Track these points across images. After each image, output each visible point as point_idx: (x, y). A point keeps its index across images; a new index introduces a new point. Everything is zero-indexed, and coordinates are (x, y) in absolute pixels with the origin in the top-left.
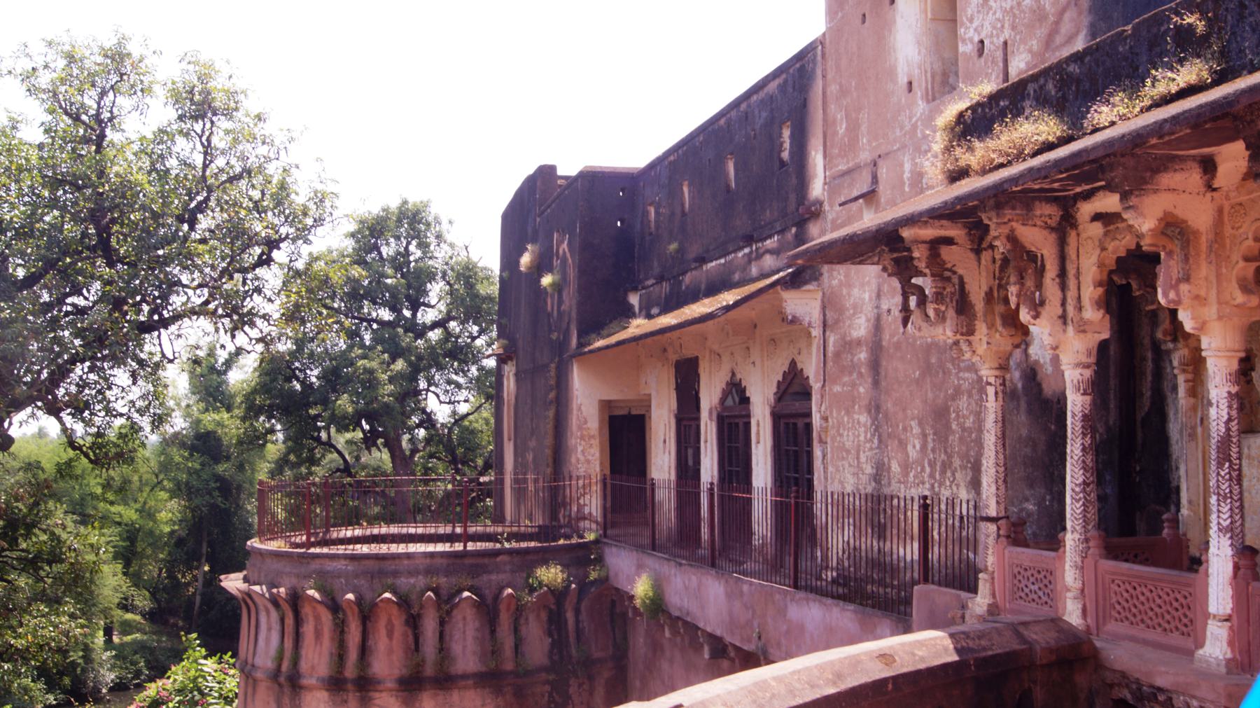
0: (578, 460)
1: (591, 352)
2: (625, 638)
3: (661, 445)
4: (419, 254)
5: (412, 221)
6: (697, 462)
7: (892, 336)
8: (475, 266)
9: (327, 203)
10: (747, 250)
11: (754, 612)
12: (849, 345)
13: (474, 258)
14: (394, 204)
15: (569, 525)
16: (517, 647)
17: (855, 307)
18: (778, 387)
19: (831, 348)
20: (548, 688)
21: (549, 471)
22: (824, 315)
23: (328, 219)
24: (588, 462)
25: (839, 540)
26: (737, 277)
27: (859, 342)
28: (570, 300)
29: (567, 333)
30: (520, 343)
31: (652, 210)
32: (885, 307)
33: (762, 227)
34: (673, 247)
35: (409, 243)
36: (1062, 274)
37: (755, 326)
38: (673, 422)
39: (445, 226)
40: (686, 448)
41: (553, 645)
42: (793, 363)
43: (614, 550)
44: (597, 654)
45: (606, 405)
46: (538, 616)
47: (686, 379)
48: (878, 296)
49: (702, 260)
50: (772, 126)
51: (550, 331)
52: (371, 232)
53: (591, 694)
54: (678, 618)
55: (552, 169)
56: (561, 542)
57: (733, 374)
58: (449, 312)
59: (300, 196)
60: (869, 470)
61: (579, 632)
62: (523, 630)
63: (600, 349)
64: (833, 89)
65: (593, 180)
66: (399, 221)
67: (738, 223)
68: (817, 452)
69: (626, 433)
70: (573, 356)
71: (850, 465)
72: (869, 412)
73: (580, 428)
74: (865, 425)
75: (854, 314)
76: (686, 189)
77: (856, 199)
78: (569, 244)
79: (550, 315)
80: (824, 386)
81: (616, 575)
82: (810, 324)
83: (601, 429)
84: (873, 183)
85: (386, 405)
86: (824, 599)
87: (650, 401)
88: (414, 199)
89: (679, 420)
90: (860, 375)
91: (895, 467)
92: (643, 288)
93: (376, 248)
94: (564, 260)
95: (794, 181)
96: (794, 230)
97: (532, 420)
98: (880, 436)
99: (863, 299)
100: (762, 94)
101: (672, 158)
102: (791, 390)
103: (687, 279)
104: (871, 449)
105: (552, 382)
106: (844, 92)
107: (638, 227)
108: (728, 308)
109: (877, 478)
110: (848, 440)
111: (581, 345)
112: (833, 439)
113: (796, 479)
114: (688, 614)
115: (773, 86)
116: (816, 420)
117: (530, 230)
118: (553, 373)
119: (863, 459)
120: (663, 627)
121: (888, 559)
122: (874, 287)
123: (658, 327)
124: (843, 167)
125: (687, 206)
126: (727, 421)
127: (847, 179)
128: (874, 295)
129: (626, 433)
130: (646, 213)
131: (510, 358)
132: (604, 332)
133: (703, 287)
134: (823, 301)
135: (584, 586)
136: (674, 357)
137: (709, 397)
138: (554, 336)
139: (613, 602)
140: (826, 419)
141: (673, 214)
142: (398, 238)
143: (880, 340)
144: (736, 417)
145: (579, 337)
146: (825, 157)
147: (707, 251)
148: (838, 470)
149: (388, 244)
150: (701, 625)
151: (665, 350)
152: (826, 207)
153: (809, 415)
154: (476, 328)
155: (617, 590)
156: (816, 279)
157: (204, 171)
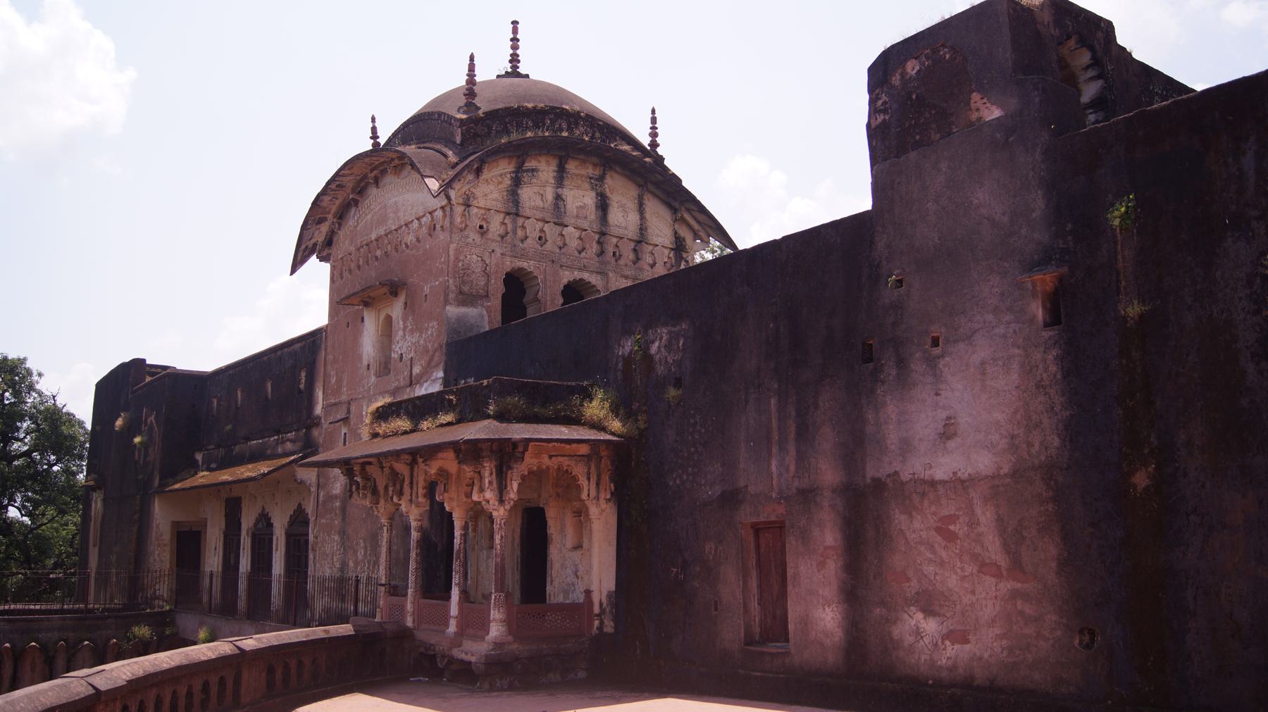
6: (237, 562)
12: (330, 498)
26: (269, 452)
31: (215, 401)
34: (229, 427)
36: (411, 483)
42: (300, 505)
45: (176, 524)
49: (248, 439)
63: (177, 490)
64: (330, 357)
68: (311, 556)
69: (188, 543)
89: (226, 536)
91: (351, 564)
94: (151, 428)
100: (291, 349)
103: (237, 448)
109: (341, 570)
111: (162, 485)
116: (311, 538)
129: (188, 543)
131: (100, 488)
137: (248, 521)
138: (140, 477)
154: (53, 457)
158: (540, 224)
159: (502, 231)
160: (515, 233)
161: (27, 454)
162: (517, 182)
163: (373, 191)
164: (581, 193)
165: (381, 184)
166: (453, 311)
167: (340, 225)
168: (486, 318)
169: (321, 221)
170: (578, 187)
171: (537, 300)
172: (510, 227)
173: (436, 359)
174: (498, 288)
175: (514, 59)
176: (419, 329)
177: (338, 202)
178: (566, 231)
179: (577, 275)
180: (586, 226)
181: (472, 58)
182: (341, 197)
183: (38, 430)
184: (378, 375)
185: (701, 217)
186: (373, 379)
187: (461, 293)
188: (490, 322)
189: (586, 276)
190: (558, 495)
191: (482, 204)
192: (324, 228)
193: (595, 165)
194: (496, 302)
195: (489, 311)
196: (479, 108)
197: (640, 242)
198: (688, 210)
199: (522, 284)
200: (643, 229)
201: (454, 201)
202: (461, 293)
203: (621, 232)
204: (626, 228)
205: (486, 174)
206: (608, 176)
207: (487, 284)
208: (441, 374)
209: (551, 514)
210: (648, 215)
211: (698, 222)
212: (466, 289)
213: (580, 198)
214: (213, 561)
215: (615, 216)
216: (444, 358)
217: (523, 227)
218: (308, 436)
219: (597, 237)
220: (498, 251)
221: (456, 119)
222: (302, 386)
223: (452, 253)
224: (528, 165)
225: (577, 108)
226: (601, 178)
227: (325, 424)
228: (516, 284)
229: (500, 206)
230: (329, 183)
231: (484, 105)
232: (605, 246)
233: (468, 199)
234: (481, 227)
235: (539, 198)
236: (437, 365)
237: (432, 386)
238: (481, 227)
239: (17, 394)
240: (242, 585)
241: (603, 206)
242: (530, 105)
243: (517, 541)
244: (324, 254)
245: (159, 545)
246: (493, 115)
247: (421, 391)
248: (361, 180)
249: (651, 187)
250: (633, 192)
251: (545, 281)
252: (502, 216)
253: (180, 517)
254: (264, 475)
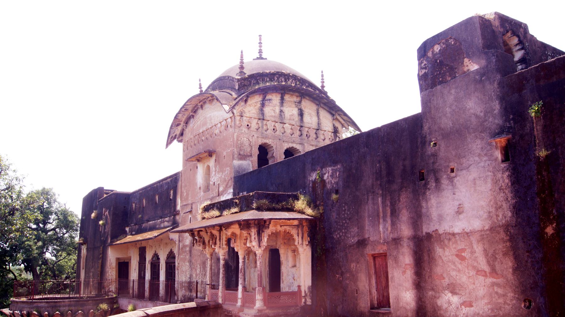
6: (145, 275)
12: (185, 246)
25: (181, 293)
27: (187, 246)
28: (108, 229)
29: (107, 238)
31: (134, 205)
34: (140, 216)
36: (220, 239)
42: (171, 250)
45: (118, 259)
49: (148, 221)
50: (168, 190)
51: (101, 237)
60: (188, 276)
63: (118, 244)
64: (183, 184)
68: (176, 272)
69: (123, 267)
73: (110, 266)
76: (144, 201)
78: (109, 212)
79: (101, 232)
89: (140, 263)
91: (194, 275)
94: (107, 217)
100: (166, 181)
103: (144, 225)
106: (186, 186)
109: (190, 278)
110: (184, 269)
111: (111, 242)
115: (169, 180)
124: (185, 203)
129: (123, 267)
131: (85, 244)
132: (119, 238)
136: (139, 246)
137: (149, 257)
138: (102, 239)
141: (140, 207)
153: (175, 263)
158: (273, 123)
159: (257, 127)
160: (263, 127)
161: (54, 229)
162: (263, 105)
163: (200, 111)
164: (291, 109)
165: (204, 108)
166: (236, 163)
167: (186, 126)
168: (251, 165)
169: (178, 125)
170: (290, 106)
171: (273, 157)
172: (260, 125)
173: (229, 184)
174: (256, 152)
175: (260, 52)
176: (221, 171)
177: (185, 117)
178: (285, 126)
179: (291, 145)
180: (294, 123)
181: (242, 52)
182: (187, 114)
183: (58, 219)
184: (205, 192)
185: (345, 118)
186: (202, 193)
187: (240, 154)
188: (253, 167)
189: (295, 146)
190: (285, 243)
191: (248, 115)
192: (180, 128)
193: (297, 96)
194: (255, 158)
195: (252, 162)
196: (245, 74)
197: (318, 130)
198: (339, 115)
199: (266, 150)
200: (319, 124)
201: (235, 115)
202: (240, 154)
203: (309, 125)
204: (311, 124)
205: (250, 102)
206: (303, 101)
207: (251, 150)
208: (232, 191)
209: (282, 252)
210: (321, 117)
211: (344, 120)
212: (242, 153)
213: (291, 111)
214: (134, 275)
215: (307, 118)
216: (233, 184)
217: (266, 125)
218: (174, 219)
219: (299, 128)
220: (256, 136)
221: (236, 79)
222: (171, 197)
223: (235, 137)
224: (267, 97)
225: (288, 72)
226: (300, 102)
227: (182, 214)
228: (264, 150)
229: (256, 116)
230: (181, 109)
231: (248, 72)
232: (303, 132)
233: (242, 113)
234: (248, 125)
235: (273, 112)
236: (230, 187)
237: (228, 196)
238: (248, 125)
239: (49, 203)
240: (147, 285)
241: (301, 114)
242: (268, 71)
243: (267, 264)
244: (180, 139)
246: (252, 76)
247: (223, 198)
248: (195, 107)
249: (322, 105)
250: (314, 107)
251: (276, 149)
252: (257, 120)
253: (120, 256)
254: (156, 237)
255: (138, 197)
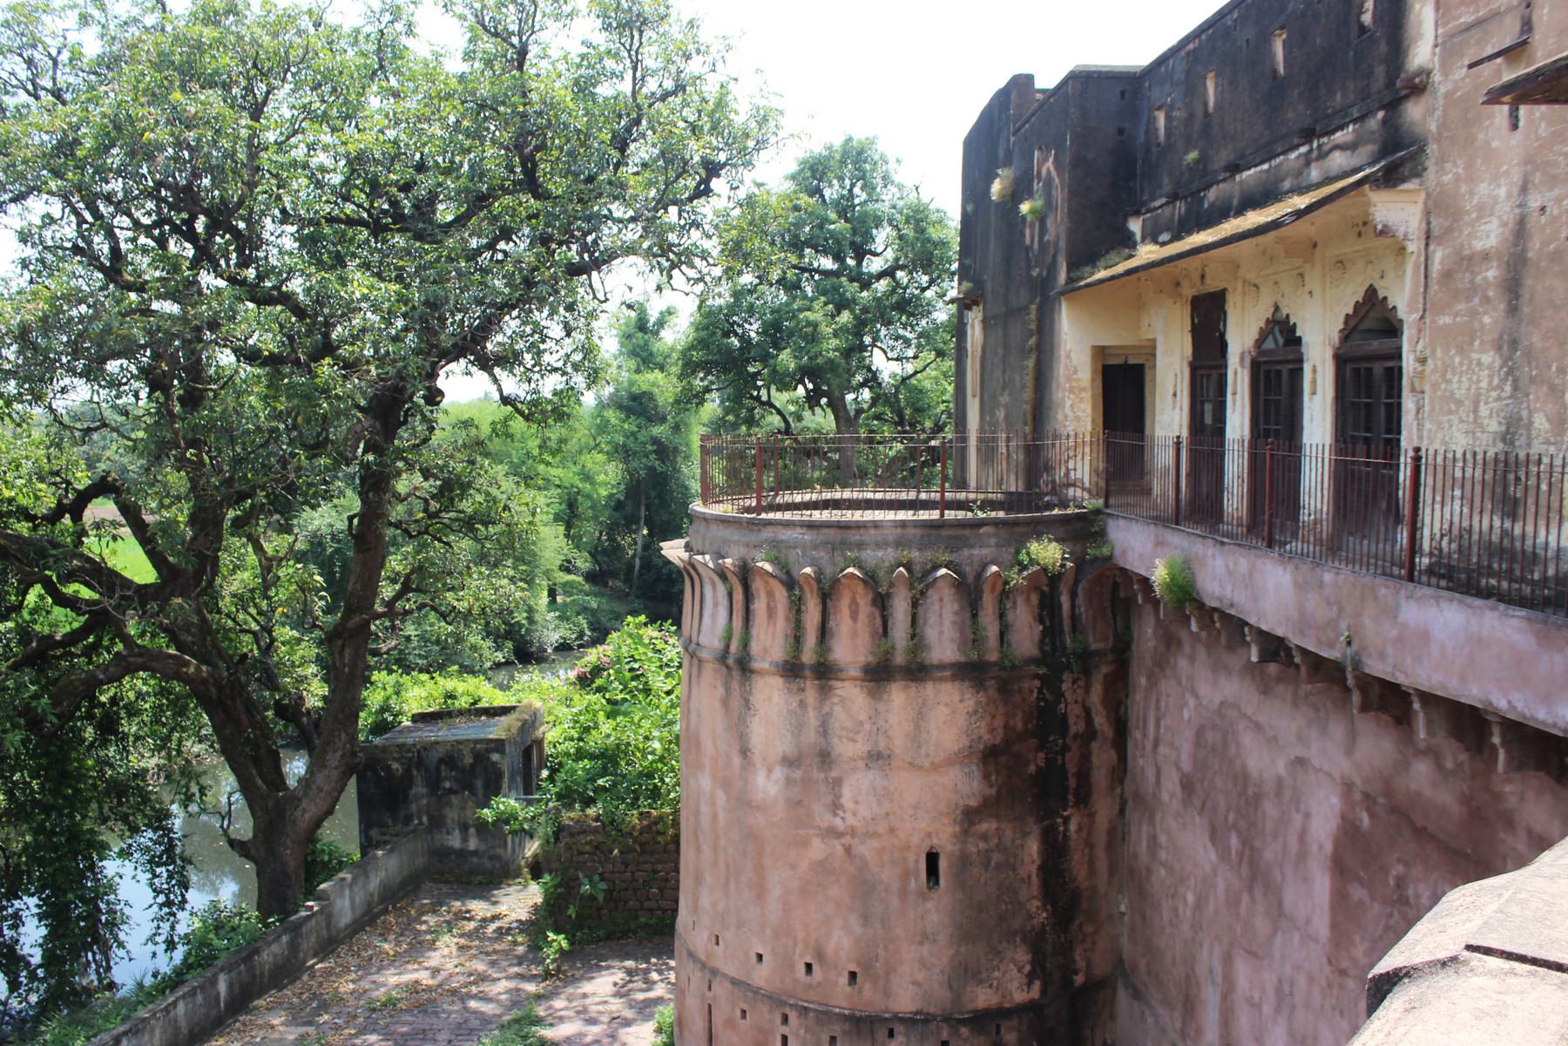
0: (1066, 417)
1: (1088, 285)
2: (1128, 627)
3: (1170, 398)
4: (864, 196)
5: (856, 160)
7: (1545, 243)
8: (926, 207)
9: (772, 123)
10: (1303, 149)
11: (1341, 610)
12: (1468, 261)
13: (925, 200)
14: (838, 143)
15: (1054, 492)
16: (1002, 634)
17: (1481, 208)
18: (1346, 323)
19: (1436, 267)
20: (1037, 683)
21: (1028, 429)
22: (1429, 223)
23: (773, 140)
24: (1078, 418)
25: (1441, 518)
26: (1287, 185)
27: (1486, 256)
28: (1057, 228)
29: (1052, 269)
30: (989, 285)
31: (1161, 118)
32: (1534, 202)
33: (1329, 116)
34: (1193, 155)
35: (853, 186)
37: (1315, 246)
38: (1187, 371)
39: (892, 166)
40: (1203, 403)
41: (1044, 633)
42: (1371, 292)
43: (1121, 522)
44: (1095, 646)
45: (1100, 352)
46: (1028, 599)
47: (1208, 318)
48: (1524, 189)
49: (1234, 169)
52: (814, 174)
53: (1087, 691)
54: (1215, 609)
55: (1029, 79)
56: (1056, 512)
57: (1277, 308)
58: (897, 259)
59: (740, 115)
60: (1494, 426)
61: (1074, 618)
62: (1010, 616)
63: (1101, 281)
65: (1084, 82)
66: (843, 162)
67: (1291, 115)
68: (1408, 403)
69: (1123, 387)
70: (1063, 293)
71: (1461, 421)
72: (1499, 349)
73: (1069, 379)
74: (1490, 367)
75: (1478, 219)
77: (1491, 58)
79: (1028, 249)
80: (1422, 317)
81: (1124, 553)
82: (1406, 235)
83: (1093, 380)
84: (1522, 32)
85: (831, 361)
86: (1469, 600)
87: (1154, 347)
88: (859, 135)
90: (1486, 300)
91: (1540, 422)
92: (1148, 211)
93: (817, 191)
94: (1049, 182)
95: (1383, 48)
96: (1381, 114)
97: (1004, 372)
98: (1515, 381)
99: (1496, 197)
101: (1191, 46)
102: (1361, 327)
103: (1212, 194)
104: (1499, 399)
105: (1033, 327)
107: (1142, 138)
108: (1299, 214)
109: (1507, 437)
110: (1460, 387)
111: (1070, 280)
112: (1435, 387)
113: (1366, 440)
114: (1232, 605)
116: (1408, 362)
117: (1001, 153)
118: (1033, 316)
119: (1484, 411)
120: (1188, 618)
121: (1518, 545)
122: (1516, 177)
123: (1187, 248)
124: (1467, 18)
125: (1211, 104)
126: (1263, 369)
127: (1476, 34)
128: (1515, 190)
129: (1123, 387)
130: (1152, 121)
131: (976, 303)
132: (1101, 263)
133: (1235, 202)
134: (1425, 204)
135: (1081, 563)
136: (1189, 292)
137: (1241, 336)
138: (1035, 273)
139: (1116, 586)
140: (1423, 361)
141: (1191, 116)
142: (841, 179)
143: (1524, 250)
144: (1279, 362)
145: (1069, 271)
146: (1437, 9)
147: (1242, 156)
148: (1440, 427)
149: (831, 186)
150: (1252, 621)
151: (1178, 284)
152: (1437, 77)
154: (925, 279)
155: (1123, 571)
156: (1419, 175)
157: (635, 99)
214: (1169, 418)
240: (1235, 466)
245: (1071, 390)
253: (1108, 340)
255: (1179, 75)
